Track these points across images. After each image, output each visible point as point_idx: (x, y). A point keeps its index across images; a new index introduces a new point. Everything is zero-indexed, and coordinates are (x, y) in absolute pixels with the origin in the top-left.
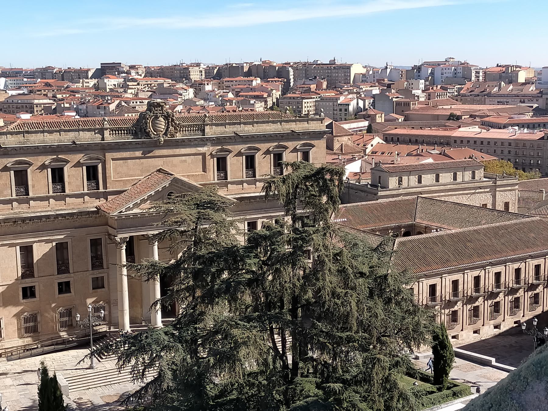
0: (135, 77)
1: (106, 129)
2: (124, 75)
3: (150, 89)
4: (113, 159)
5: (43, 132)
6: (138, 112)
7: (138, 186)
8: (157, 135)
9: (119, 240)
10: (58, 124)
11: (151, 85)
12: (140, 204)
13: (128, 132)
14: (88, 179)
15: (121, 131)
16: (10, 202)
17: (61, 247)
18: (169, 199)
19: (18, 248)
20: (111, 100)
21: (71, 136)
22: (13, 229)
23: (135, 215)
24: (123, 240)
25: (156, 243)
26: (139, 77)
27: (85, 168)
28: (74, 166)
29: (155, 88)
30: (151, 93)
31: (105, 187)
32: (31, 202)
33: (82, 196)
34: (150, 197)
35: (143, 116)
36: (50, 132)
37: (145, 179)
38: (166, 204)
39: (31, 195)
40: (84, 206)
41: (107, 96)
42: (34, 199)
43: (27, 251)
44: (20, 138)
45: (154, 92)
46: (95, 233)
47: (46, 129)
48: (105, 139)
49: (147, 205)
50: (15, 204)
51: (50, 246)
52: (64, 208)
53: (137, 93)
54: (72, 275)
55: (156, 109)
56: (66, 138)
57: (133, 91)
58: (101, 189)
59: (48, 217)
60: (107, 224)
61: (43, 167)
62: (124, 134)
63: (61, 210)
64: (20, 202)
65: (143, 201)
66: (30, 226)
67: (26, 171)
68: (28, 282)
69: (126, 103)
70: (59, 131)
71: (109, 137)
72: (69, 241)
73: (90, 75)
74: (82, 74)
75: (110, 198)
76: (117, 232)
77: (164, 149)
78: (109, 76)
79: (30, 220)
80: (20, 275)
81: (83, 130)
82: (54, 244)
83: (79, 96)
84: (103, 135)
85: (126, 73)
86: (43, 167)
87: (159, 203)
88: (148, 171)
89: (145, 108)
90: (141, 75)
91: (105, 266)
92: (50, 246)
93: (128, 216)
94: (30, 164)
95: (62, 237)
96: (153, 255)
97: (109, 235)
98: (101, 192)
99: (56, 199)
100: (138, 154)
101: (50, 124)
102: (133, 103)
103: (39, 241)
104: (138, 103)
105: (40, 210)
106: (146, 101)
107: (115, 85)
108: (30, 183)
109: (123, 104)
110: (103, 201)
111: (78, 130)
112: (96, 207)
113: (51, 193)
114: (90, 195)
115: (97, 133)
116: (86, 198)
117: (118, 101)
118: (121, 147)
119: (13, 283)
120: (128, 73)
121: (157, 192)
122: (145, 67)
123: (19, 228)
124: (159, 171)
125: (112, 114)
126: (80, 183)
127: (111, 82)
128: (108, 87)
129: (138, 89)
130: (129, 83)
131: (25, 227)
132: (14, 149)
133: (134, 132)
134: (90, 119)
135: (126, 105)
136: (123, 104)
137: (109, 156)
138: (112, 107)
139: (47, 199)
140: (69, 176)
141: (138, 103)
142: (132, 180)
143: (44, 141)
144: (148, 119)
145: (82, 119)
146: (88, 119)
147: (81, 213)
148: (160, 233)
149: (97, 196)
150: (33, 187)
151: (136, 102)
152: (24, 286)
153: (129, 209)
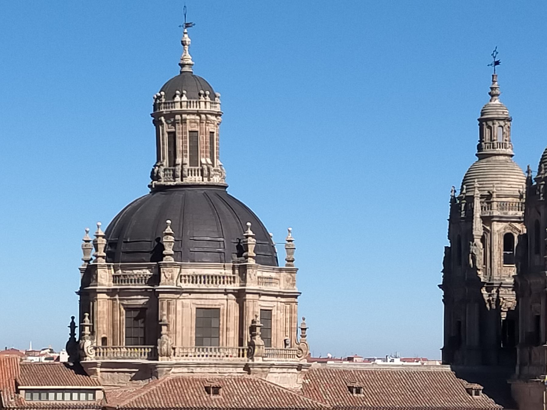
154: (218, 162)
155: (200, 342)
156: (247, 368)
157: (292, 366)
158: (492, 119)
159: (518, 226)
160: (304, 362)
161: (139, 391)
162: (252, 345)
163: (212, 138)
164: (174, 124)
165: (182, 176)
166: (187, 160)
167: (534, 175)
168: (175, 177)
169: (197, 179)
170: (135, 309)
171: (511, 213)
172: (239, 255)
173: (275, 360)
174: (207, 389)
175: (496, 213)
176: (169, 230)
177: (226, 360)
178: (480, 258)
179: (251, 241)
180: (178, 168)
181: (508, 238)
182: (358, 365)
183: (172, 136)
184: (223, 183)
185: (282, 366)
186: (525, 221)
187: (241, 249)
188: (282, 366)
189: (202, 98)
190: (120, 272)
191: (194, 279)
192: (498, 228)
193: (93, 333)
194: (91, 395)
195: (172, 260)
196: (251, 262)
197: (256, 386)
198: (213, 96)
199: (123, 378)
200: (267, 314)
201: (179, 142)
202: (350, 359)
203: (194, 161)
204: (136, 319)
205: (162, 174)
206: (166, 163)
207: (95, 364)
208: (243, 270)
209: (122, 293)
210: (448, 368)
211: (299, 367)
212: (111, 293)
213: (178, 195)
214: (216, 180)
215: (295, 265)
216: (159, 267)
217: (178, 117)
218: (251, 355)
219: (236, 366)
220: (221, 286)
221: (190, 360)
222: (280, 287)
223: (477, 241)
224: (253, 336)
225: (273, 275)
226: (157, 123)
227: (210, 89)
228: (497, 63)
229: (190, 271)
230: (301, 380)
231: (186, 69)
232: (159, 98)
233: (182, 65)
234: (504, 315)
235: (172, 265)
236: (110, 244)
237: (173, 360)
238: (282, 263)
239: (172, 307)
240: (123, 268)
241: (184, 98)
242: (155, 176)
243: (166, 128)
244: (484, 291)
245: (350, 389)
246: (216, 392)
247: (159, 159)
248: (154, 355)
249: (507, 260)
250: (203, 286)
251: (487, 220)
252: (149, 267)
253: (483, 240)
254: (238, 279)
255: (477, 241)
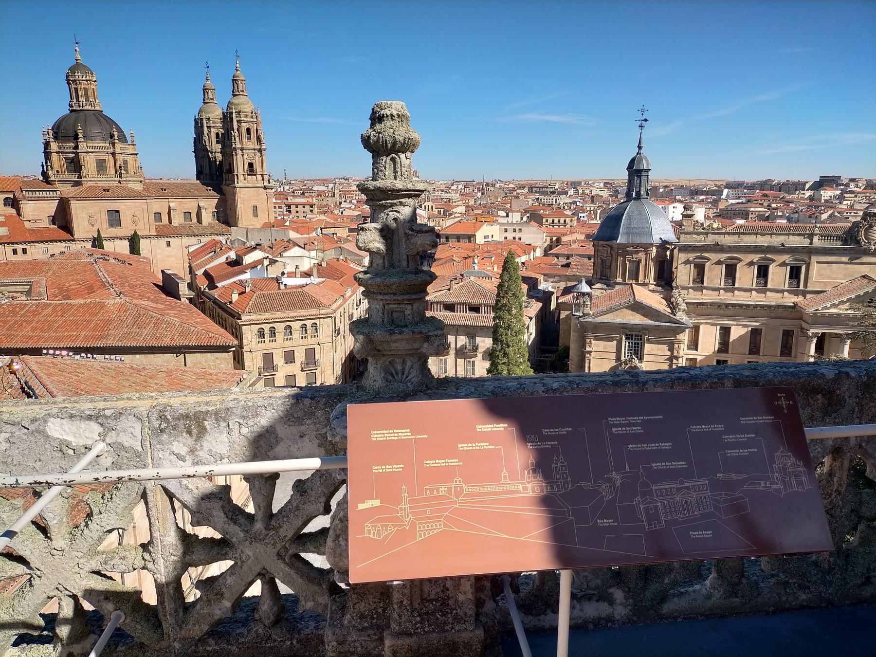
0: (853, 189)
1: (816, 235)
2: (842, 187)
3: (867, 201)
4: (818, 262)
5: (756, 234)
6: (849, 222)
7: (839, 289)
8: (868, 243)
9: (811, 334)
10: (771, 228)
11: (869, 197)
12: (838, 305)
13: (838, 238)
14: (791, 277)
15: (834, 237)
16: (718, 289)
17: (755, 333)
18: (869, 302)
19: (718, 327)
20: (824, 210)
21: (781, 239)
22: (717, 311)
23: (831, 315)
24: (815, 335)
25: (849, 341)
26: (858, 189)
27: (789, 268)
28: (780, 265)
29: (873, 200)
30: (869, 205)
31: (806, 285)
32: (736, 292)
33: (781, 291)
34: (848, 300)
35: (856, 225)
36: (763, 235)
37: (848, 283)
38: (866, 307)
39: (737, 285)
40: (783, 300)
41: (821, 206)
42: (739, 290)
43: (725, 331)
44: (736, 238)
45: (872, 204)
46: (789, 325)
47: (759, 231)
48: (813, 244)
49: (847, 305)
50: (722, 292)
51: (746, 330)
52: (764, 300)
53: (853, 204)
54: (761, 357)
55: (872, 218)
56: (776, 241)
57: (849, 202)
58: (801, 287)
59: (748, 306)
60: (801, 319)
61: (751, 264)
62: (833, 240)
63: (761, 301)
64: (726, 290)
65: (843, 303)
66: (731, 311)
67: (736, 266)
68: (722, 357)
69: (839, 213)
70: (771, 234)
71: (817, 242)
72: (764, 328)
73: (807, 187)
74: (799, 186)
75: (808, 296)
76: (810, 326)
77: (873, 257)
78: (826, 188)
79: (732, 307)
80: (716, 349)
81: (793, 234)
82: (750, 329)
83: (793, 205)
84: (812, 240)
85: (845, 185)
86: (751, 264)
87: (860, 306)
88: (852, 276)
89: (859, 219)
90: (860, 188)
91: (793, 354)
92: (746, 330)
93: (823, 315)
94: (740, 260)
95: (758, 324)
96: (843, 352)
97: (802, 328)
98: (800, 290)
99: (758, 291)
100: (845, 259)
101: (763, 228)
102: (847, 213)
103: (737, 325)
104: (852, 214)
105: (742, 299)
106: (861, 213)
107: (830, 196)
108: (738, 275)
109: (836, 214)
110: (801, 298)
111: (789, 234)
112: (793, 303)
113: (754, 286)
114: (790, 292)
115: (806, 238)
116: (786, 294)
117: (831, 212)
118: (828, 252)
119: (710, 355)
120: (847, 185)
121: (858, 297)
122: (866, 180)
123: (722, 312)
124: (864, 277)
125: (824, 222)
126: (782, 280)
127: (826, 194)
128: (823, 198)
129: (855, 201)
130: (846, 195)
131: (727, 312)
132: (729, 247)
133: (844, 239)
134: (802, 225)
135: (839, 215)
136: (836, 214)
137: (814, 259)
138: (824, 217)
139: (750, 290)
140: (773, 273)
141: (852, 214)
142: (834, 282)
143: (755, 242)
144: (861, 227)
145: (794, 225)
146: (800, 225)
147: (778, 307)
148: (854, 333)
149: (796, 294)
150: (740, 279)
151: (850, 213)
152: (719, 358)
153: (826, 308)
154: (97, 101)
155: (98, 172)
156: (120, 182)
157: (138, 181)
158: (208, 89)
159: (220, 130)
160: (143, 180)
161: (76, 191)
162: (120, 173)
163: (94, 91)
164: (76, 84)
165: (83, 106)
166: (84, 100)
167: (225, 111)
168: (79, 106)
169: (90, 108)
170: (69, 159)
171: (217, 125)
172: (111, 138)
173: (131, 179)
174: (104, 190)
175: (212, 125)
176: (80, 128)
177: (110, 179)
178: (207, 142)
179: (115, 133)
180: (81, 103)
181: (217, 134)
182: (164, 181)
183: (76, 89)
184: (101, 109)
185: (134, 181)
186: (223, 128)
187: (112, 136)
188: (134, 181)
189: (87, 74)
190: (60, 144)
191: (93, 147)
192: (212, 130)
193: (52, 168)
194: (55, 193)
195: (83, 140)
196: (116, 141)
197: (124, 188)
198: (92, 74)
199: (68, 186)
200: (125, 162)
201: (79, 92)
202: (161, 179)
203: (87, 100)
204: (70, 163)
205: (73, 105)
206: (75, 100)
207: (55, 181)
208: (113, 144)
209: (62, 152)
210: (198, 182)
211: (141, 182)
212: (58, 152)
213: (81, 114)
214: (97, 108)
215: (135, 143)
216: (77, 142)
217: (78, 82)
218: (120, 177)
219: (115, 181)
220: (105, 150)
221: (96, 179)
222: (130, 151)
223: (206, 135)
224: (121, 170)
225: (126, 146)
226: (69, 84)
227: (90, 70)
228: (208, 67)
229: (91, 145)
230: (142, 186)
231: (79, 61)
232: (68, 73)
233: (77, 60)
234: (218, 163)
235: (83, 142)
236: (55, 133)
237: (88, 179)
238: (130, 142)
239: (85, 158)
240: (61, 143)
241: (79, 74)
242: (71, 106)
243: (73, 86)
244: (210, 154)
245: (162, 189)
246: (108, 191)
247: (71, 99)
248: (80, 177)
249: (218, 142)
250: (97, 150)
251: (209, 127)
252: (73, 142)
253: (208, 135)
254: (112, 148)
255: (206, 135)
